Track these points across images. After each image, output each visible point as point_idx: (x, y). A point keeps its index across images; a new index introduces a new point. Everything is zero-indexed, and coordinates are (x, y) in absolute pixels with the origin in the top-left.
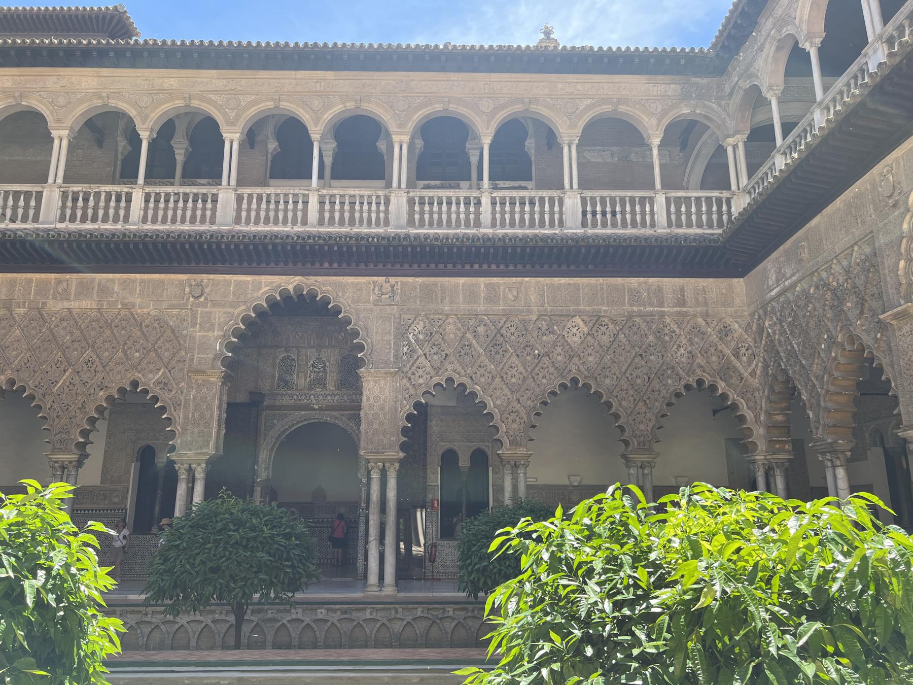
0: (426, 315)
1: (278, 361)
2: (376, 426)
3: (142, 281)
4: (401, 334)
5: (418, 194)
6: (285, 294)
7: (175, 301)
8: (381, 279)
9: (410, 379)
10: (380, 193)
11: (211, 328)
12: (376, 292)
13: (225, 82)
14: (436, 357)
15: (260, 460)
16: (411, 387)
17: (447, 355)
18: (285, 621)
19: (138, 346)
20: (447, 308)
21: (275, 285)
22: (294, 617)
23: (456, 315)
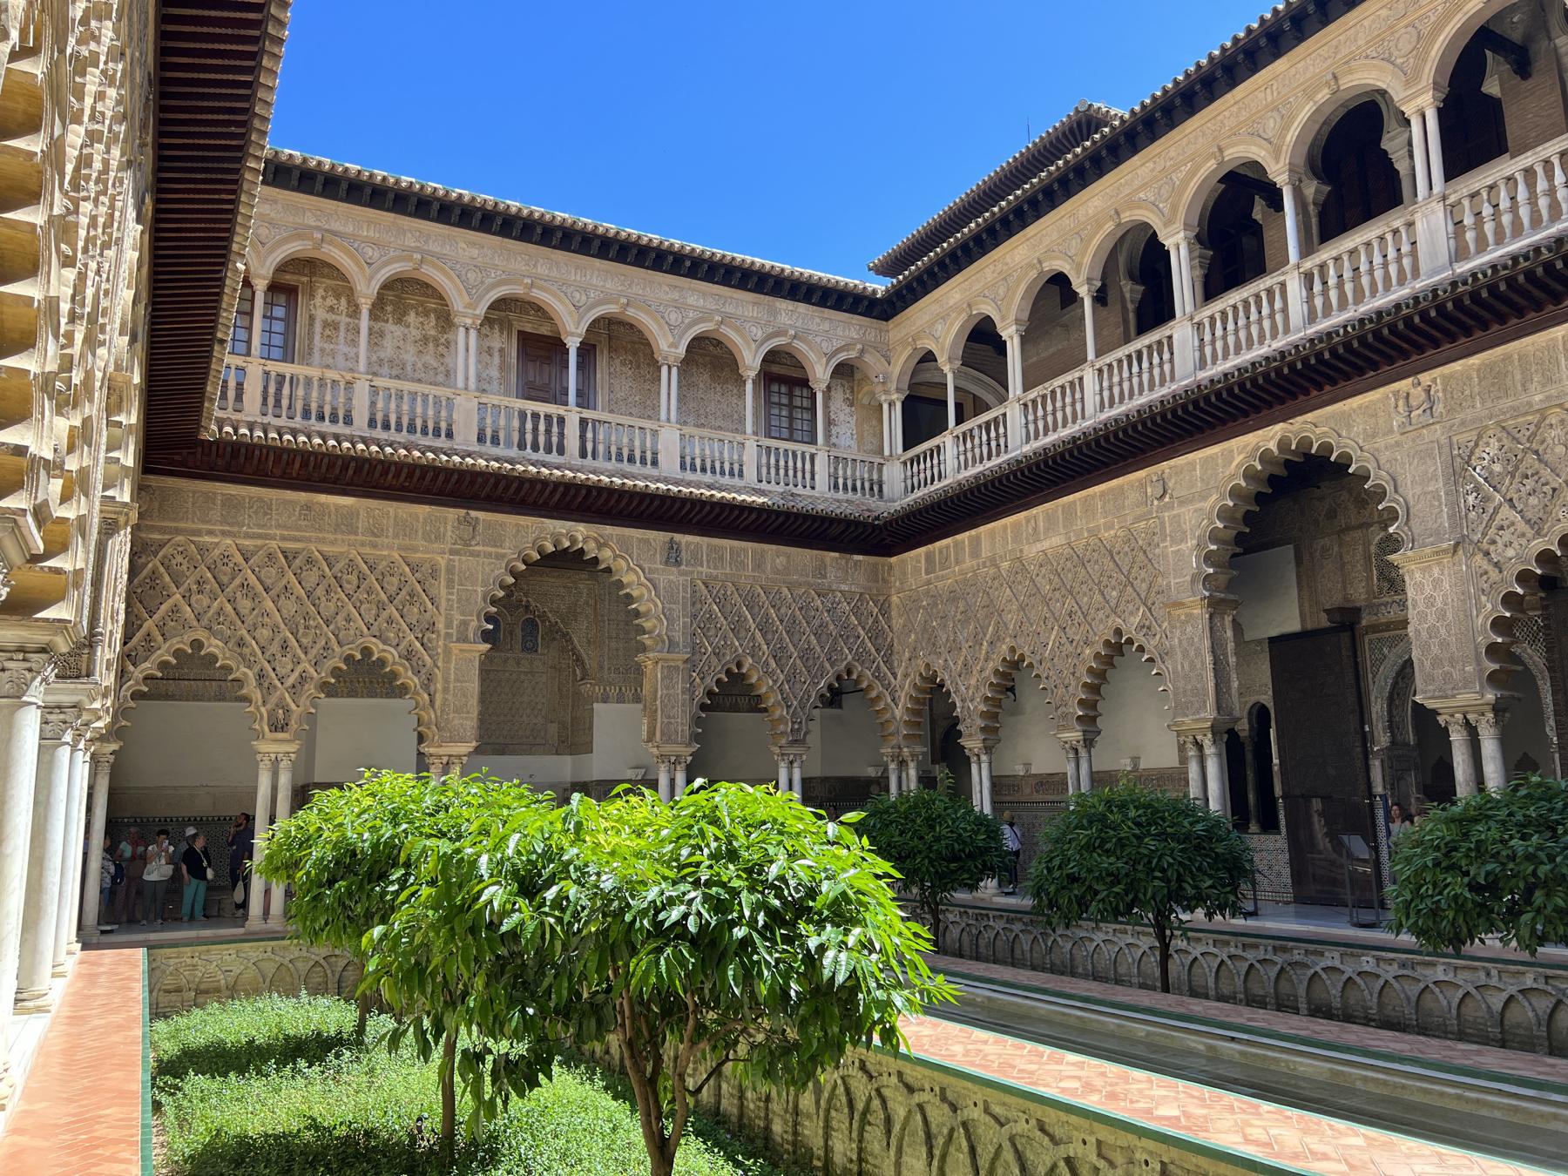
0: (1498, 423)
1: (1373, 549)
2: (1435, 650)
3: (1102, 494)
4: (1458, 469)
5: (1465, 192)
6: (1265, 457)
7: (1139, 511)
8: (1404, 385)
9: (1487, 554)
10: (1397, 223)
11: (1183, 540)
12: (1401, 409)
13: (1150, 165)
14: (1533, 500)
15: (1374, 716)
16: (1490, 568)
17: (1554, 490)
18: (1318, 969)
19: (1113, 582)
20: (1537, 398)
21: (1249, 449)
22: (1330, 964)
23: (1560, 406)
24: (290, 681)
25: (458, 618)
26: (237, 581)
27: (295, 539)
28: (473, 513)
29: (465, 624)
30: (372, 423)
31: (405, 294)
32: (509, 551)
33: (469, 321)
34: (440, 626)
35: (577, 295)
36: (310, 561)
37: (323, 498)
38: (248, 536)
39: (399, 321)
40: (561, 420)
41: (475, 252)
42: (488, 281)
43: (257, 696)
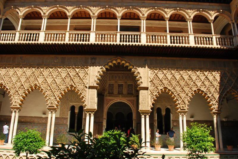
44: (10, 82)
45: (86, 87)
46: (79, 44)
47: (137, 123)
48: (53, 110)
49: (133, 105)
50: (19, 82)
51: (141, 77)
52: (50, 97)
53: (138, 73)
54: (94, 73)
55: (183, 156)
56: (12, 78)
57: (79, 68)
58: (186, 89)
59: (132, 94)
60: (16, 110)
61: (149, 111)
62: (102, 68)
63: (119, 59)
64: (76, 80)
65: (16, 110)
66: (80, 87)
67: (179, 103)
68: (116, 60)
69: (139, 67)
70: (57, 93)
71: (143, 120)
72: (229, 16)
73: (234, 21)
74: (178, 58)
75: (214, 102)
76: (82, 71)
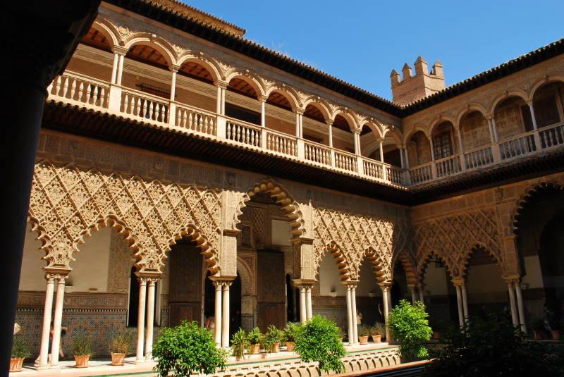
24: (457, 259)
25: (504, 228)
26: (438, 231)
27: (450, 214)
28: (501, 187)
29: (506, 230)
30: (468, 167)
31: (473, 119)
32: (517, 197)
33: (490, 117)
34: (499, 232)
35: (525, 86)
36: (456, 220)
37: (454, 198)
38: (438, 217)
39: (480, 126)
40: (532, 136)
41: (484, 93)
42: (492, 99)
43: (449, 266)
44: (42, 201)
45: (218, 231)
46: (155, 126)
47: (258, 303)
48: (152, 278)
49: (251, 267)
50: (66, 205)
51: (303, 221)
52: (147, 249)
53: (300, 212)
54: (232, 203)
55: (364, 353)
56: (47, 192)
57: (205, 190)
58: (358, 247)
59: (250, 247)
60: (59, 277)
61: (313, 281)
62: (244, 196)
63: (271, 181)
64: (200, 215)
65: (59, 277)
66: (208, 231)
67: (349, 269)
68: (266, 184)
69: (300, 203)
70: (162, 239)
71: (219, 295)
72: (400, 138)
73: (405, 147)
74: (348, 195)
75: (386, 269)
76: (209, 197)
